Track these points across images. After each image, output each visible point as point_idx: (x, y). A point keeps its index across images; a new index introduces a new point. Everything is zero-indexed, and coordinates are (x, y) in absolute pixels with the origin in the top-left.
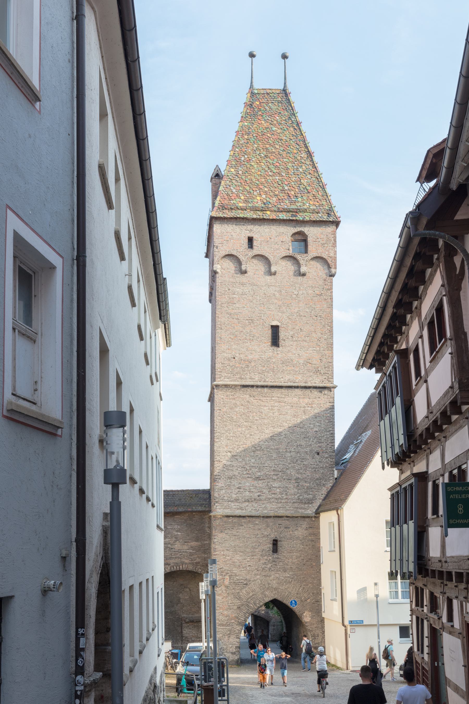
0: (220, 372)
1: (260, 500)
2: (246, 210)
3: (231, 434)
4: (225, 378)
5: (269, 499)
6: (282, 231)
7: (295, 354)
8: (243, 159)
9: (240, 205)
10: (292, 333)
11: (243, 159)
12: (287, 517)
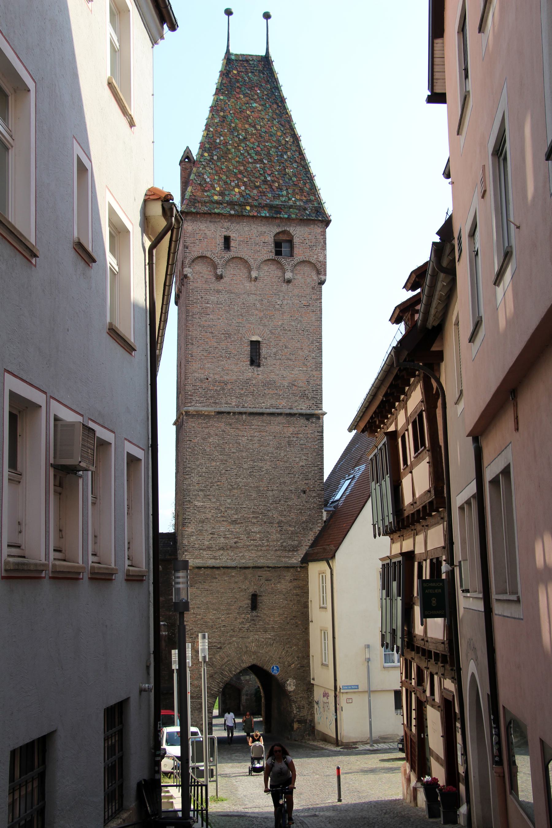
0: (190, 395)
1: (237, 547)
2: (221, 204)
3: (204, 470)
4: (196, 403)
5: (248, 546)
6: (264, 230)
7: (278, 375)
8: (218, 141)
9: (216, 198)
10: (274, 350)
11: (218, 141)
12: (268, 567)
